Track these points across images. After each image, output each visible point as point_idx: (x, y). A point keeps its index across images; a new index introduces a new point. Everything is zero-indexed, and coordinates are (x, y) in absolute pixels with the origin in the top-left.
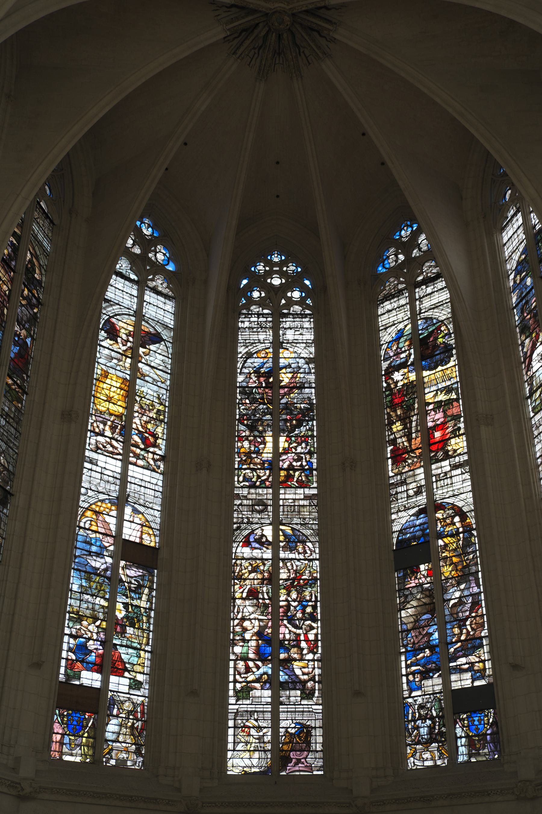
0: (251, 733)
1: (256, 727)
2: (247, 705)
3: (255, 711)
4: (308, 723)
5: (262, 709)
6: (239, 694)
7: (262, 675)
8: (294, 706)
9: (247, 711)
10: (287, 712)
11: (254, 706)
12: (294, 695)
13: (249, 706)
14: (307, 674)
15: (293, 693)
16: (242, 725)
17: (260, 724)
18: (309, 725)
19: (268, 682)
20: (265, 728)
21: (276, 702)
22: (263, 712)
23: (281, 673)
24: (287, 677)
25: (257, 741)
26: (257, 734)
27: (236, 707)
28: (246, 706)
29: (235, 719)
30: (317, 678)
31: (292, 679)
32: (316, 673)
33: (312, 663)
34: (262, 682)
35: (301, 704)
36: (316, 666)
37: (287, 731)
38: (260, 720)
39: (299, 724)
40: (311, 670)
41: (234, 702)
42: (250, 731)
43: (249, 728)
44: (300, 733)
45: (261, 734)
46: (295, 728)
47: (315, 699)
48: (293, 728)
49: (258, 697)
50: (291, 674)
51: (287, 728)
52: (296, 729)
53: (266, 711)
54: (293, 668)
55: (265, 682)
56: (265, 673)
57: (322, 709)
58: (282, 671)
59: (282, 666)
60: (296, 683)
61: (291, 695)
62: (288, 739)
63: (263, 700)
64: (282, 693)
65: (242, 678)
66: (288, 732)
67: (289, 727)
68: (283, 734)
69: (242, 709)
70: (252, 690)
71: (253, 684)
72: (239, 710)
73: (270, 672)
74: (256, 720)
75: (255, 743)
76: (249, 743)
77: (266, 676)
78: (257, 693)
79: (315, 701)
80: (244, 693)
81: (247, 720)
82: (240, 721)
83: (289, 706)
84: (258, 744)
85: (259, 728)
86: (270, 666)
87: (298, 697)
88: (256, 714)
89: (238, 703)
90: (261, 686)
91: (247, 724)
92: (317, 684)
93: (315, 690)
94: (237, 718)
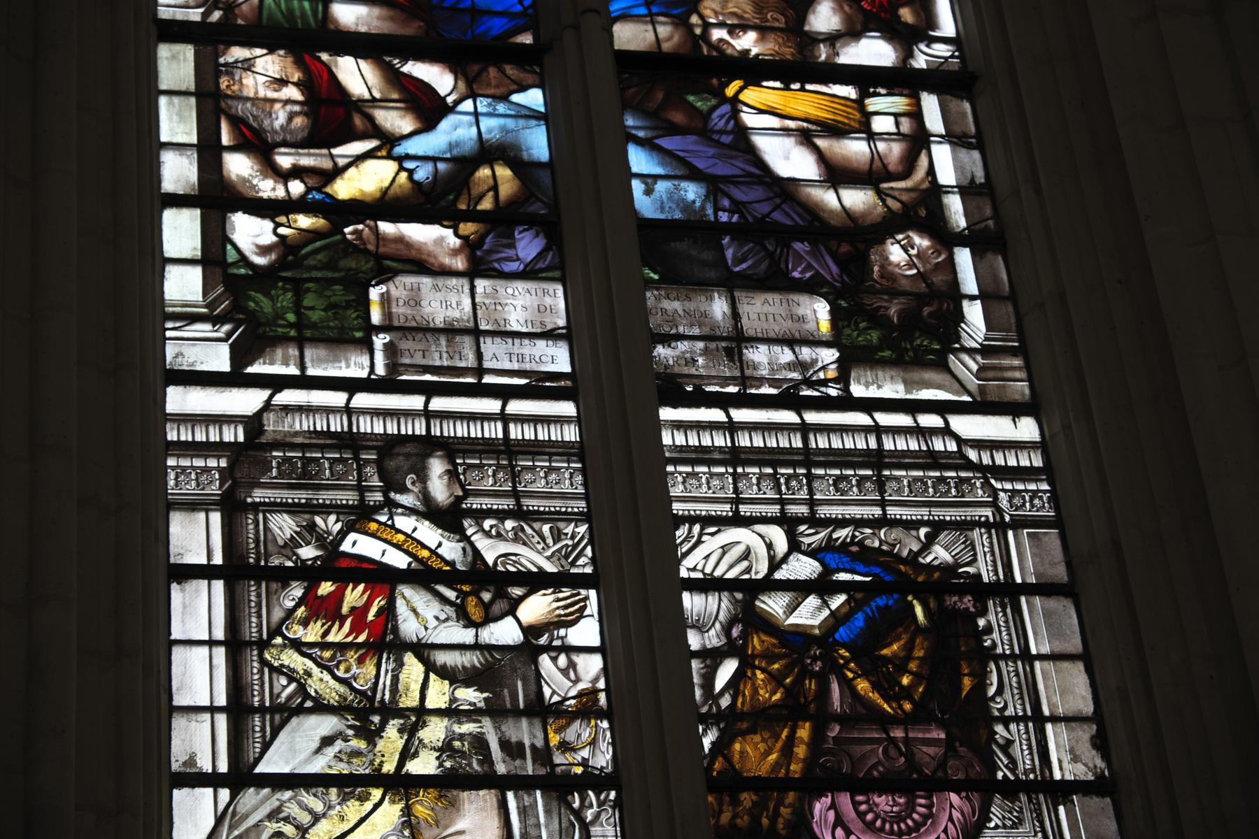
0: (409, 627)
1: (451, 576)
2: (351, 386)
3: (429, 444)
4: (940, 554)
5: (494, 431)
6: (261, 303)
7: (463, 164)
8: (788, 417)
9: (350, 442)
10: (735, 457)
11: (416, 402)
12: (776, 329)
13: (362, 400)
14: (872, 176)
15: (760, 310)
16: (308, 552)
17: (490, 551)
18: (949, 570)
19: (532, 222)
20: (536, 581)
21: (617, 384)
22: (508, 450)
23: (639, 161)
24: (692, 192)
25: (470, 696)
26: (466, 636)
27: (247, 401)
28: (337, 398)
29: (233, 507)
30: (955, 205)
31: (737, 206)
32: (947, 175)
33: (898, 103)
34: (472, 215)
35: (847, 403)
36: (934, 120)
37: (749, 618)
38: (479, 515)
39: (860, 555)
40: (893, 151)
41: (218, 359)
42: (389, 612)
43: (380, 577)
44: (878, 632)
45: (505, 632)
46: (822, 586)
47: (966, 367)
48: (800, 589)
49: (451, 331)
50: (721, 169)
51: (750, 589)
52: (838, 601)
53: (535, 449)
54: (743, 132)
55: (504, 220)
56: (488, 152)
57: (1042, 446)
58: (647, 144)
59: (639, 110)
60: (785, 235)
61: (750, 325)
62: (776, 680)
63: (496, 354)
64: (667, 306)
65: (284, 176)
66: (766, 624)
67: (770, 585)
68: (713, 638)
69: (302, 424)
70: (384, 274)
71: (386, 227)
72: (271, 424)
73: (537, 143)
74: (448, 518)
75: (451, 712)
76: (390, 711)
77: (503, 172)
78: (445, 302)
79: (973, 382)
80: (310, 290)
81: (359, 517)
82: (284, 526)
83: (740, 415)
84: (487, 727)
85: (482, 589)
86: (534, 98)
87: (815, 342)
88: (437, 467)
89: (256, 368)
90: (470, 246)
91: (361, 545)
92: (964, 257)
93: (955, 296)
94: (259, 495)
